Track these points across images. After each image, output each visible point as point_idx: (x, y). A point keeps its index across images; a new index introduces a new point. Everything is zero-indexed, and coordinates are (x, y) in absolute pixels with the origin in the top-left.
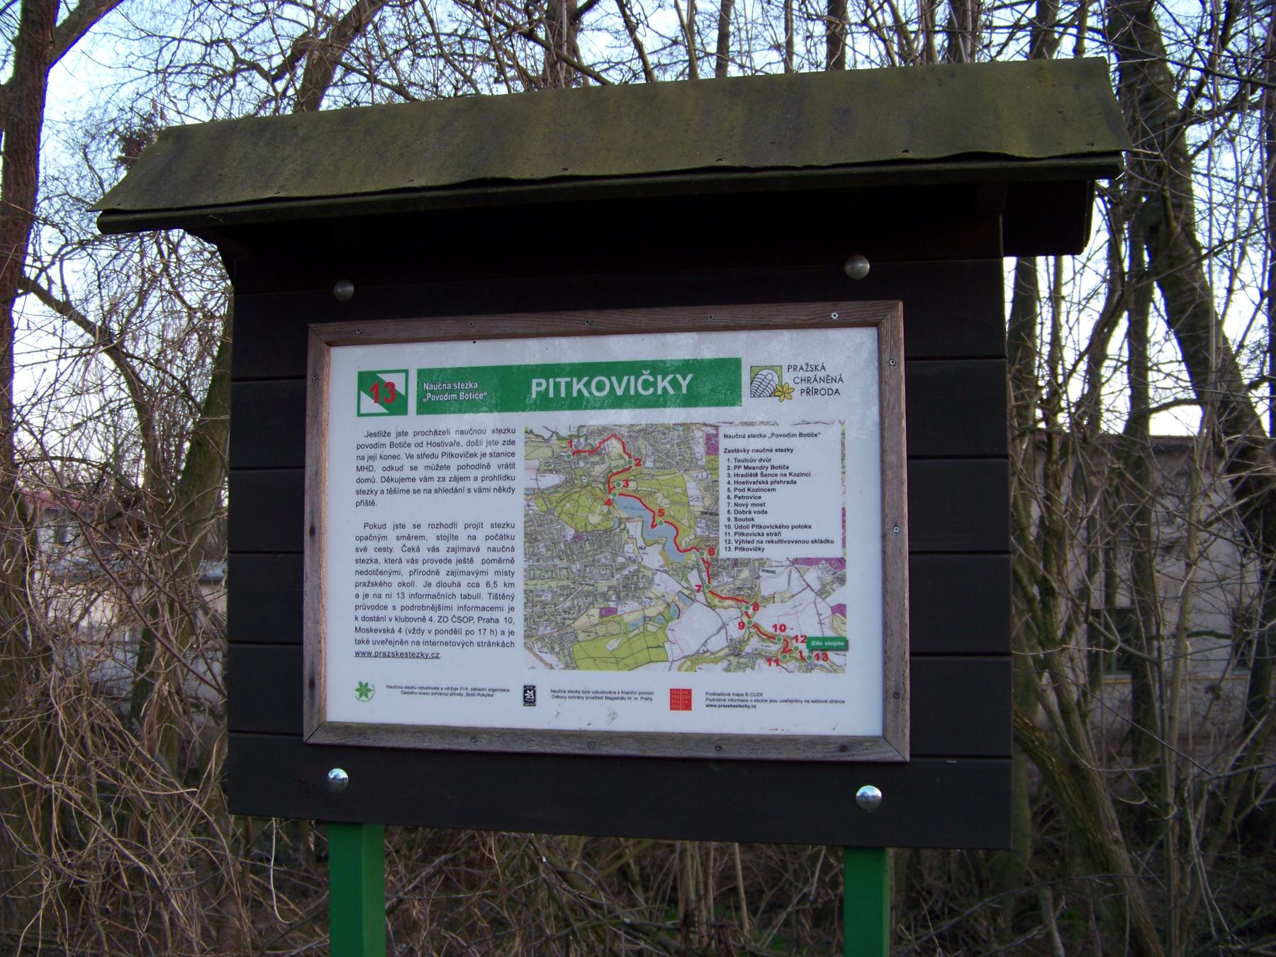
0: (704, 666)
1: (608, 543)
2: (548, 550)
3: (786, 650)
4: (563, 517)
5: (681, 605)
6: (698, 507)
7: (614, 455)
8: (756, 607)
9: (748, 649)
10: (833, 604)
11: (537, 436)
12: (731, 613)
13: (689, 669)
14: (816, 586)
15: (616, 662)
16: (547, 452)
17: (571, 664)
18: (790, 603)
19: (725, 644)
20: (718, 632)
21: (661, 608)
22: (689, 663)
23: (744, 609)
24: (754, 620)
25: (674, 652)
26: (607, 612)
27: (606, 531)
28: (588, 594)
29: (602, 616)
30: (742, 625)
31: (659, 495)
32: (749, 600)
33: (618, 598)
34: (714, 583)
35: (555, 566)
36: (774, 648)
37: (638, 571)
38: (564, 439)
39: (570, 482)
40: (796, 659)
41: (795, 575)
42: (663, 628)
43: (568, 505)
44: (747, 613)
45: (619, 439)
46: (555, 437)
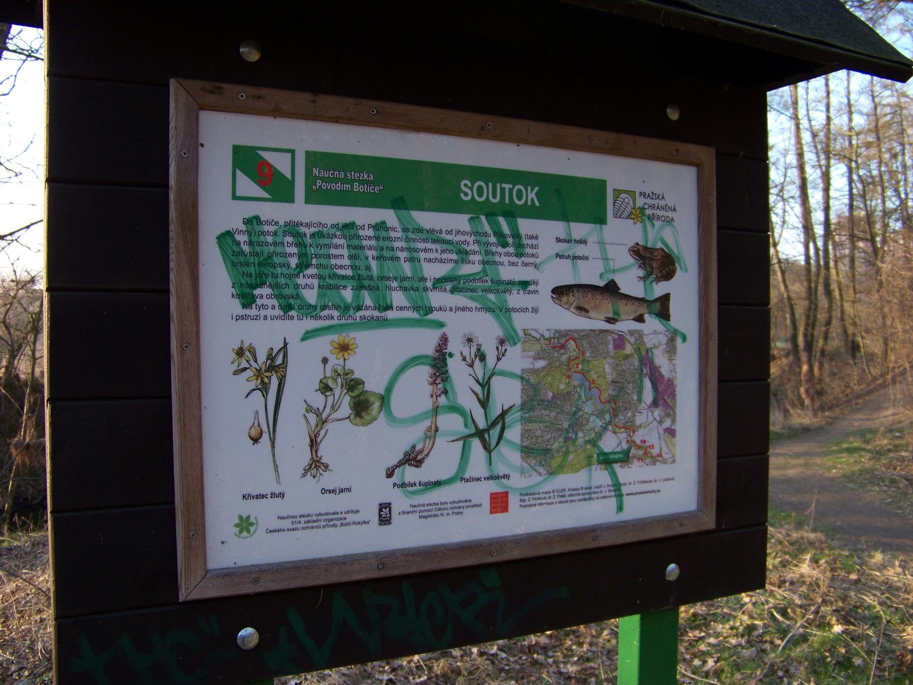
3: (645, 453)
6: (609, 378)
7: (571, 350)
8: (634, 432)
12: (623, 436)
14: (658, 418)
16: (537, 347)
24: (633, 438)
26: (567, 439)
29: (565, 442)
30: (628, 442)
32: (630, 428)
36: (641, 452)
37: (582, 415)
39: (550, 365)
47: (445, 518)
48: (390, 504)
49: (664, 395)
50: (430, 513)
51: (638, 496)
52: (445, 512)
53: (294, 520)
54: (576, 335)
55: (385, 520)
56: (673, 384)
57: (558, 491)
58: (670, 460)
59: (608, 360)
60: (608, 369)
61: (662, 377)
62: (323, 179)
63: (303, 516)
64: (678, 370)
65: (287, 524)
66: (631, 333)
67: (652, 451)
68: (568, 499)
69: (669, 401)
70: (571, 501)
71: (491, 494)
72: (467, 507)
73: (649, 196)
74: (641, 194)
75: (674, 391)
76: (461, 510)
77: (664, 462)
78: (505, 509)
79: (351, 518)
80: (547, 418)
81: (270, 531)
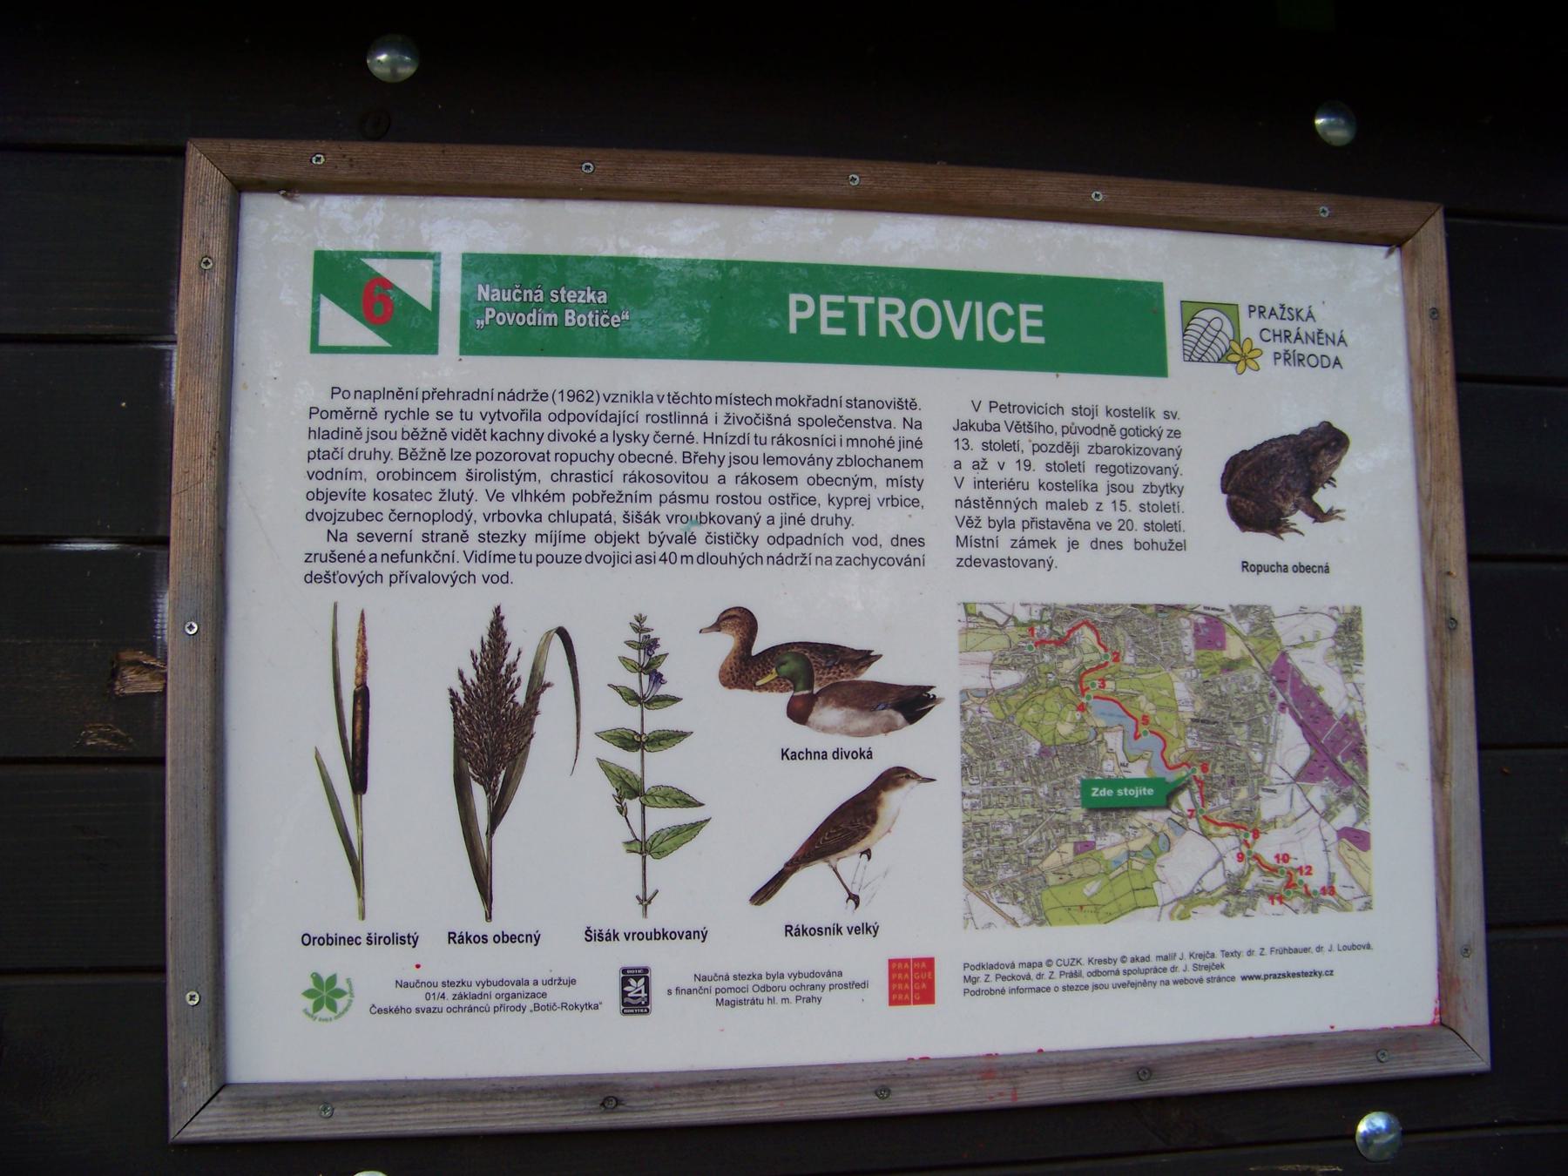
1: (1082, 759)
2: (1007, 768)
3: (1290, 885)
4: (1026, 726)
5: (1171, 835)
6: (1187, 713)
7: (1086, 648)
8: (1256, 834)
9: (1248, 886)
11: (989, 620)
12: (1228, 843)
13: (1183, 917)
14: (1320, 806)
15: (1098, 911)
16: (1002, 642)
17: (1040, 918)
18: (1293, 827)
19: (1222, 880)
20: (1214, 867)
21: (1147, 839)
22: (1181, 907)
25: (1164, 893)
26: (1084, 848)
27: (1079, 744)
28: (1059, 825)
29: (1076, 853)
30: (1240, 857)
31: (1142, 698)
32: (1248, 825)
33: (1097, 829)
34: (1209, 807)
35: (1015, 790)
36: (1277, 883)
38: (1024, 625)
39: (1033, 680)
40: (1301, 895)
41: (1298, 794)
42: (1151, 864)
43: (1031, 711)
45: (1092, 628)
46: (1011, 623)
47: (779, 1008)
48: (646, 970)
49: (1337, 752)
50: (741, 996)
51: (1271, 981)
52: (779, 995)
53: (432, 990)
54: (1097, 617)
55: (635, 1003)
56: (1356, 726)
57: (1061, 962)
59: (1182, 671)
60: (1182, 691)
61: (1328, 712)
62: (498, 306)
63: (452, 984)
64: (1366, 691)
65: (415, 998)
66: (1241, 611)
67: (1306, 879)
68: (1090, 981)
69: (1347, 766)
70: (1096, 987)
71: (891, 961)
72: (832, 987)
73: (1273, 312)
74: (1251, 309)
75: (1362, 743)
76: (817, 993)
77: (1342, 907)
78: (927, 996)
79: (556, 994)
80: (1028, 798)
81: (380, 1011)
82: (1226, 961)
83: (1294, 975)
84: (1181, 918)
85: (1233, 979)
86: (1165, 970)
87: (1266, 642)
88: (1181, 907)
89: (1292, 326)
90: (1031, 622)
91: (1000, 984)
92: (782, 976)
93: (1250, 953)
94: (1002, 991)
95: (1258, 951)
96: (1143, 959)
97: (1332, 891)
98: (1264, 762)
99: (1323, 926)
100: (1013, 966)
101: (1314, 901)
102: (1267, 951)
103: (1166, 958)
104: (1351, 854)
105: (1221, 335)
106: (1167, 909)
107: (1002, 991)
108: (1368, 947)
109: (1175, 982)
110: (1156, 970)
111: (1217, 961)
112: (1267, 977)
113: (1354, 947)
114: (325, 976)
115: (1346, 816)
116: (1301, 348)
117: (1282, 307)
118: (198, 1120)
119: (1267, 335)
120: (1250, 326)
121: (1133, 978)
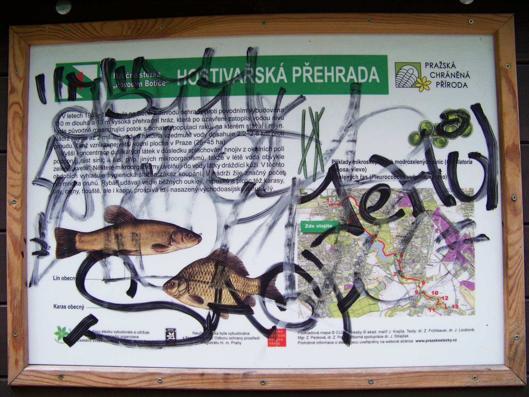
0: (398, 313)
1: (348, 252)
3: (438, 304)
5: (386, 283)
8: (423, 283)
9: (419, 304)
10: (460, 281)
14: (453, 272)
21: (376, 284)
23: (417, 284)
27: (347, 245)
36: (433, 303)
38: (325, 197)
40: (443, 308)
41: (442, 267)
44: (419, 286)
47: (225, 345)
48: (175, 330)
51: (429, 343)
58: (469, 312)
72: (245, 339)
74: (427, 64)
76: (239, 341)
77: (461, 313)
82: (409, 334)
83: (439, 341)
84: (390, 316)
85: (412, 341)
86: (382, 337)
87: (430, 204)
88: (390, 312)
89: (445, 71)
90: (328, 196)
91: (313, 340)
92: (226, 334)
93: (420, 331)
94: (314, 343)
95: (423, 331)
96: (373, 332)
97: (457, 307)
98: (428, 253)
99: (454, 321)
100: (318, 333)
101: (448, 310)
102: (427, 330)
103: (383, 332)
104: (466, 292)
105: (413, 76)
106: (385, 312)
107: (314, 343)
108: (473, 330)
109: (387, 342)
110: (378, 337)
111: (405, 334)
112: (427, 341)
113: (466, 330)
114: (62, 328)
115: (464, 276)
116: (448, 80)
117: (441, 63)
118: (17, 377)
119: (433, 75)
120: (426, 72)
121: (368, 340)
